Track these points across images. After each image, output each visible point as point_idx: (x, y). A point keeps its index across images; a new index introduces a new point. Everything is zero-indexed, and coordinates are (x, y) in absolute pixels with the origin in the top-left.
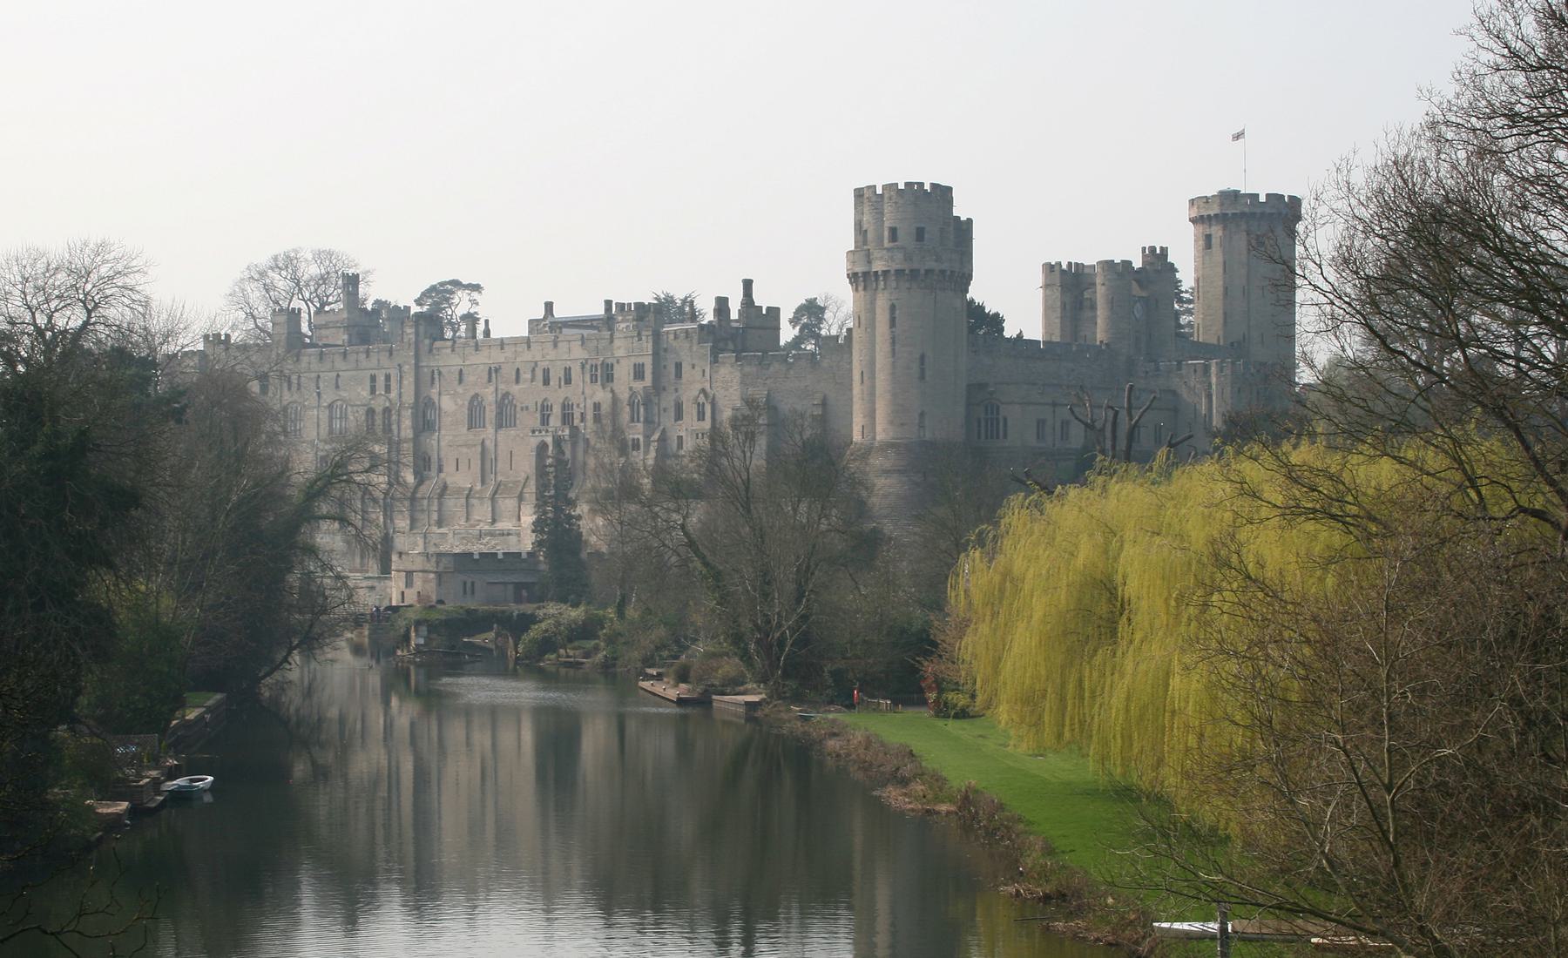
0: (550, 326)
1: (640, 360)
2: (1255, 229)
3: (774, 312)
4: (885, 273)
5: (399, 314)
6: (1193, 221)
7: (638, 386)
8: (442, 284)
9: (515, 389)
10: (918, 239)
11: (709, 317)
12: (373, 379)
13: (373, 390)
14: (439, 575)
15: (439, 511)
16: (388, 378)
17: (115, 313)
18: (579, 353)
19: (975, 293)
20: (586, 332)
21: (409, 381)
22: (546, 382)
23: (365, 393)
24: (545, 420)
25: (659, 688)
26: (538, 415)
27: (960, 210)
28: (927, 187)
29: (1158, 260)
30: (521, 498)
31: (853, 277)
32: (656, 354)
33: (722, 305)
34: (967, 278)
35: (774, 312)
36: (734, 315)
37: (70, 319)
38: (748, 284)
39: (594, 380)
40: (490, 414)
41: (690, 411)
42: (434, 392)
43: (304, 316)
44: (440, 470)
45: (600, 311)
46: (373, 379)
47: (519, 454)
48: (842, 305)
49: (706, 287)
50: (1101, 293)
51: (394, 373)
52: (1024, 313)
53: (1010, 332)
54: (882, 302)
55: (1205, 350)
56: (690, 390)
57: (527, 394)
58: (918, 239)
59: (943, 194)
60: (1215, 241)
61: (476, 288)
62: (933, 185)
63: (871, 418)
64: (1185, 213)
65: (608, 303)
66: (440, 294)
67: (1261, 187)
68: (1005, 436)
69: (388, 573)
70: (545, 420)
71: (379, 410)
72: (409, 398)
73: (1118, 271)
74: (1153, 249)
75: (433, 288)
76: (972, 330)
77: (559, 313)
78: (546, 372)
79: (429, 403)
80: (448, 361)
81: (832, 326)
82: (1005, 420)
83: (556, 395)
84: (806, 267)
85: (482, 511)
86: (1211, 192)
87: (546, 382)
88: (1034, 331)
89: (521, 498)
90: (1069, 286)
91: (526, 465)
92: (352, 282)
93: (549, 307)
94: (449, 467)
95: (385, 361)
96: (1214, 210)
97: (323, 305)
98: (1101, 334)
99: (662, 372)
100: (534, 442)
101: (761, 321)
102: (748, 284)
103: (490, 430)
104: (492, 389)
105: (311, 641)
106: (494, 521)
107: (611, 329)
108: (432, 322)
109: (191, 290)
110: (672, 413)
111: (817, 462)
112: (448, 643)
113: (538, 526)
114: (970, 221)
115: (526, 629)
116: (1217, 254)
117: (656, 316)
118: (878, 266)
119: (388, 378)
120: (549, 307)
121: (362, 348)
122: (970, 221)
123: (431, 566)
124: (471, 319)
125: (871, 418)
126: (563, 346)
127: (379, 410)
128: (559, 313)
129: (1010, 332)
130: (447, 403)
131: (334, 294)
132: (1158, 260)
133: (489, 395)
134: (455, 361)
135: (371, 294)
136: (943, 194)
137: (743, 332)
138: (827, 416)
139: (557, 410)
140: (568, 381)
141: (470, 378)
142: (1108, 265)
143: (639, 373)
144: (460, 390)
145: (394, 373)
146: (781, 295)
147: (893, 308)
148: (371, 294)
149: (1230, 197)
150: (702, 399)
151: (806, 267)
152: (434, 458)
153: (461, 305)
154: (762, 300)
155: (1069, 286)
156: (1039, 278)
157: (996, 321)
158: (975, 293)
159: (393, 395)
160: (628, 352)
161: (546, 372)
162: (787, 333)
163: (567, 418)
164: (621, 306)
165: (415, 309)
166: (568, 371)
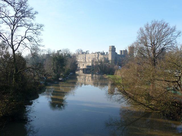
5: (84, 52)
10: (113, 49)
17: (68, 52)
19: (116, 52)
29: (126, 51)
34: (115, 51)
37: (66, 52)
47: (91, 60)
48: (109, 52)
49: (101, 51)
50: (123, 52)
52: (119, 53)
53: (118, 54)
57: (91, 57)
59: (114, 46)
63: (110, 58)
66: (87, 51)
73: (124, 51)
80: (87, 55)
83: (93, 57)
84: (107, 50)
88: (119, 54)
90: (121, 51)
91: (91, 61)
105: (79, 70)
108: (86, 53)
109: (73, 51)
111: (107, 61)
112: (87, 71)
113: (91, 64)
117: (98, 53)
125: (110, 58)
129: (118, 54)
132: (126, 51)
133: (89, 57)
135: (83, 51)
136: (114, 46)
137: (103, 54)
138: (108, 58)
146: (105, 52)
151: (107, 50)
153: (88, 52)
155: (121, 51)
158: (116, 52)
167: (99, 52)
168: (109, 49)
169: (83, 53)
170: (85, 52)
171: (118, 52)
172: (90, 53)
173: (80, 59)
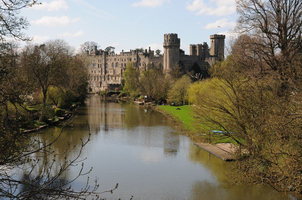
0: (123, 53)
1: (135, 58)
2: (219, 39)
3: (153, 51)
4: (168, 46)
5: (102, 51)
6: (210, 38)
7: (135, 61)
8: (109, 47)
9: (118, 62)
10: (173, 41)
11: (144, 52)
14: (108, 87)
15: (108, 78)
18: (127, 57)
21: (104, 60)
22: (122, 61)
23: (98, 62)
24: (122, 66)
25: (137, 102)
27: (179, 37)
28: (174, 34)
30: (119, 77)
31: (164, 47)
32: (137, 57)
33: (146, 50)
35: (153, 51)
36: (148, 51)
38: (150, 47)
39: (129, 60)
40: (115, 65)
41: (142, 65)
42: (107, 62)
43: (90, 52)
44: (108, 72)
45: (130, 51)
50: (197, 49)
52: (188, 52)
54: (168, 50)
55: (212, 56)
56: (142, 62)
57: (120, 62)
58: (173, 41)
59: (176, 35)
60: (213, 41)
61: (114, 48)
62: (175, 34)
64: (209, 37)
65: (131, 50)
66: (108, 49)
67: (220, 34)
69: (97, 87)
70: (122, 66)
71: (100, 65)
72: (104, 63)
73: (200, 46)
74: (205, 43)
75: (107, 48)
76: (180, 53)
78: (122, 59)
79: (107, 64)
81: (161, 53)
83: (124, 63)
84: (157, 45)
85: (114, 78)
86: (213, 34)
87: (122, 61)
89: (119, 77)
90: (193, 47)
92: (96, 47)
93: (123, 50)
94: (109, 72)
96: (213, 37)
97: (92, 50)
98: (198, 54)
99: (138, 59)
101: (151, 53)
102: (150, 47)
103: (115, 67)
104: (115, 62)
106: (115, 79)
107: (131, 53)
114: (180, 39)
115: (119, 94)
116: (214, 43)
117: (137, 51)
118: (167, 45)
120: (123, 50)
121: (98, 56)
122: (180, 39)
123: (107, 86)
124: (113, 52)
126: (125, 56)
127: (100, 65)
130: (109, 64)
131: (94, 48)
133: (115, 62)
134: (110, 57)
135: (98, 49)
136: (176, 35)
137: (149, 54)
138: (161, 66)
139: (124, 64)
140: (125, 61)
141: (112, 60)
142: (199, 45)
143: (135, 59)
145: (102, 59)
146: (154, 49)
147: (169, 51)
148: (98, 49)
149: (216, 35)
151: (157, 45)
152: (107, 71)
153: (112, 50)
154: (152, 49)
155: (193, 47)
156: (189, 47)
157: (183, 52)
158: (181, 48)
160: (134, 58)
161: (122, 59)
162: (155, 54)
163: (125, 66)
165: (105, 51)
166: (125, 59)
167: (141, 50)
168: (163, 41)
169: (98, 53)
170: (104, 49)
171: (186, 48)
172: (117, 52)
173: (94, 70)
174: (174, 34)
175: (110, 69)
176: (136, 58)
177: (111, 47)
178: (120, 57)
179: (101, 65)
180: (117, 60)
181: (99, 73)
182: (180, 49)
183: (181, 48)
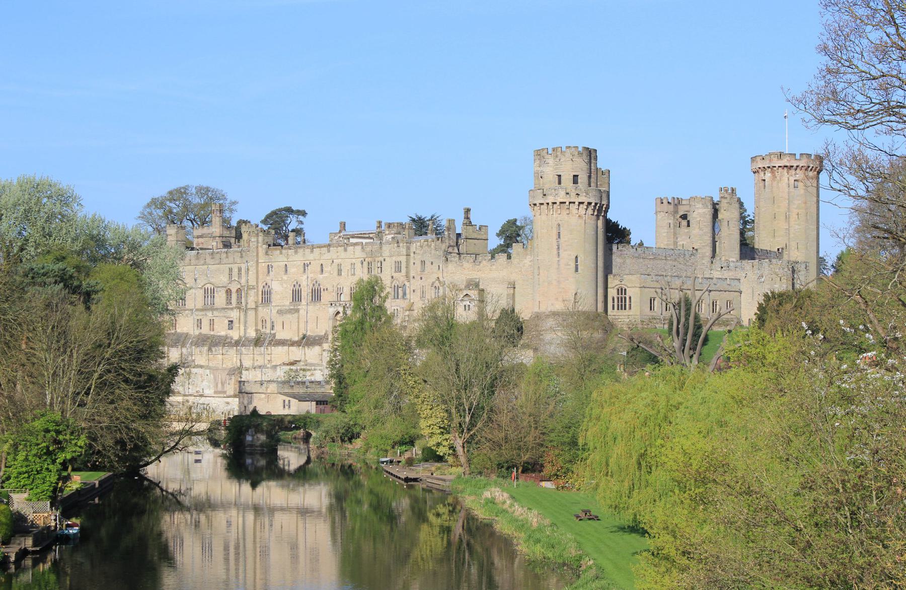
1: (399, 259)
8: (280, 210)
9: (320, 277)
12: (231, 270)
13: (230, 275)
16: (240, 270)
20: (364, 241)
21: (252, 273)
22: (340, 272)
23: (223, 279)
26: (335, 294)
33: (451, 222)
38: (468, 211)
45: (373, 228)
46: (231, 270)
51: (243, 266)
61: (304, 213)
68: (630, 308)
71: (234, 290)
77: (350, 230)
78: (339, 265)
82: (630, 298)
87: (340, 272)
93: (343, 225)
94: (278, 327)
95: (238, 260)
100: (332, 310)
104: (305, 277)
110: (418, 293)
119: (240, 270)
120: (343, 225)
128: (350, 230)
130: (276, 286)
141: (291, 270)
144: (285, 277)
150: (437, 284)
153: (293, 223)
159: (243, 281)
164: (389, 226)
174: (580, 149)
175: (280, 312)
176: (403, 259)
177: (289, 210)
178: (327, 256)
179: (239, 291)
180: (315, 267)
181: (230, 331)
182: (608, 222)
183: (612, 216)
